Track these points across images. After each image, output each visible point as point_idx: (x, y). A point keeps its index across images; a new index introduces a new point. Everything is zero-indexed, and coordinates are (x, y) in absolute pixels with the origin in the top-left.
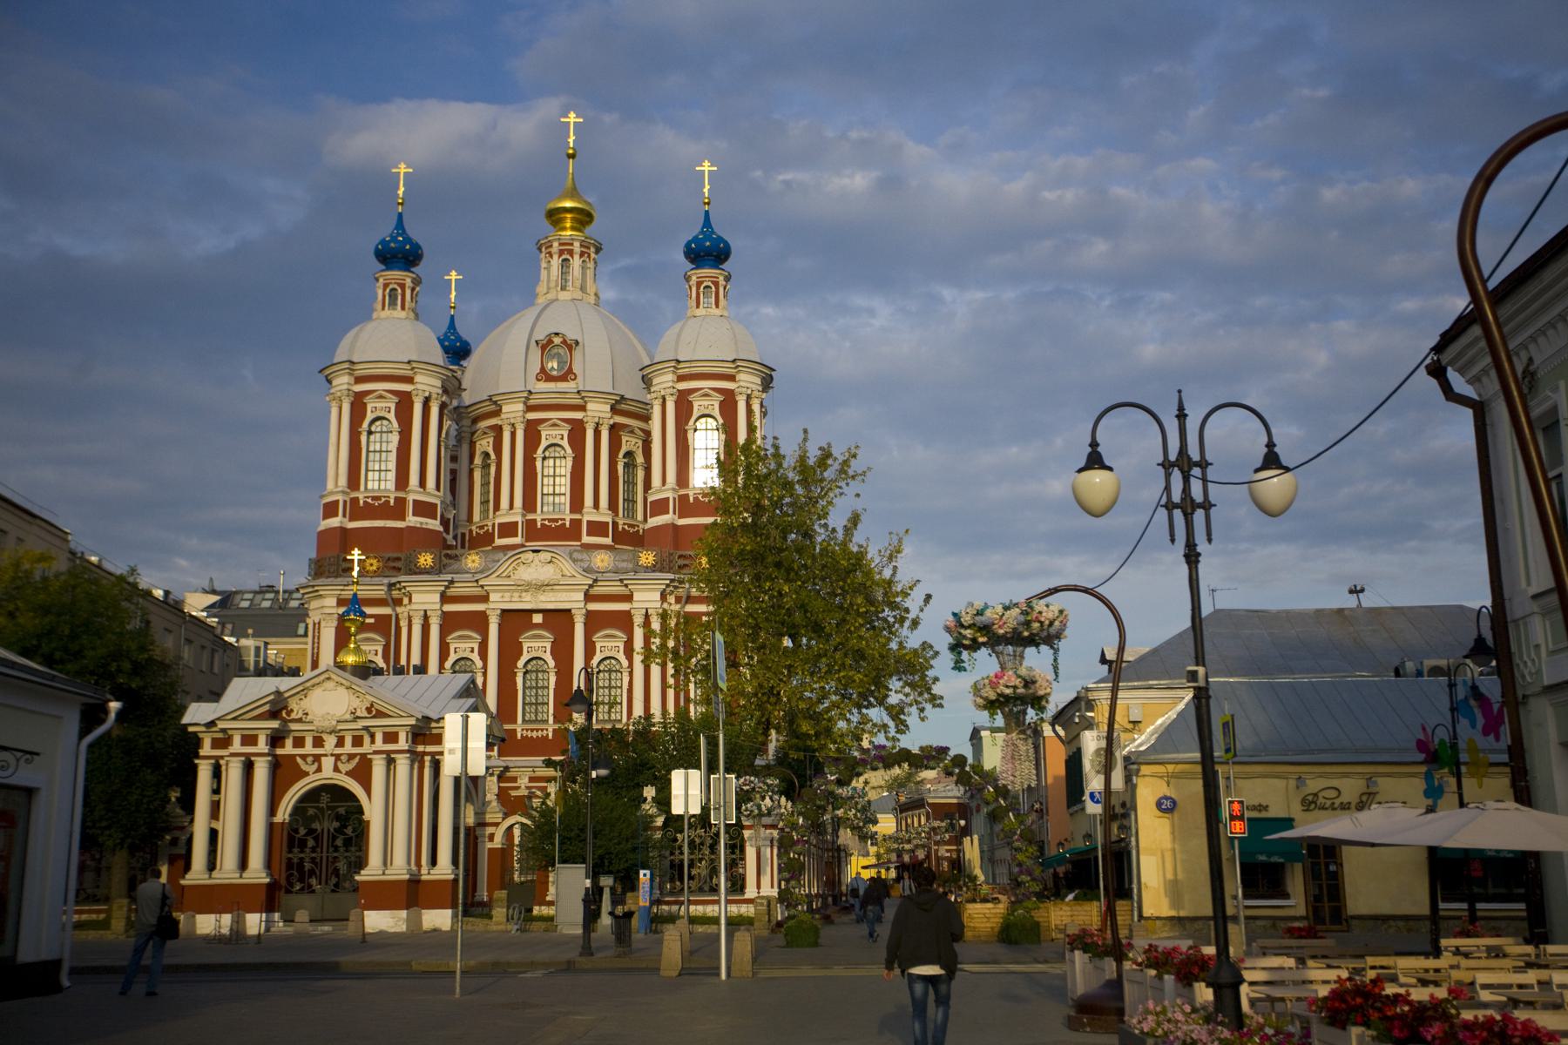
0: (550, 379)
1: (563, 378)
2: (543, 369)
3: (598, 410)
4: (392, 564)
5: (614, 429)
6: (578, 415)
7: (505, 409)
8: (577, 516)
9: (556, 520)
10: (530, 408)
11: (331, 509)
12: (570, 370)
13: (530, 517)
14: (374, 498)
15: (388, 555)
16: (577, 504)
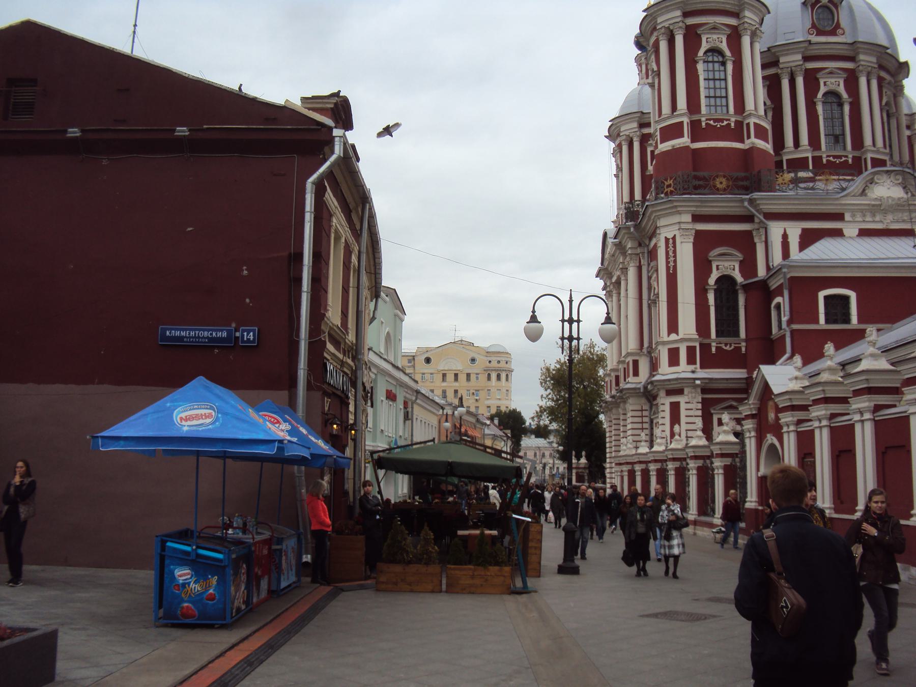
0: (820, 33)
1: (833, 33)
2: (814, 26)
3: (866, 59)
4: (741, 183)
5: (880, 80)
6: (849, 65)
7: (782, 60)
8: (857, 154)
9: (840, 157)
10: (806, 59)
11: (673, 131)
12: (838, 26)
13: (817, 154)
14: (715, 120)
15: (736, 174)
16: (858, 142)
